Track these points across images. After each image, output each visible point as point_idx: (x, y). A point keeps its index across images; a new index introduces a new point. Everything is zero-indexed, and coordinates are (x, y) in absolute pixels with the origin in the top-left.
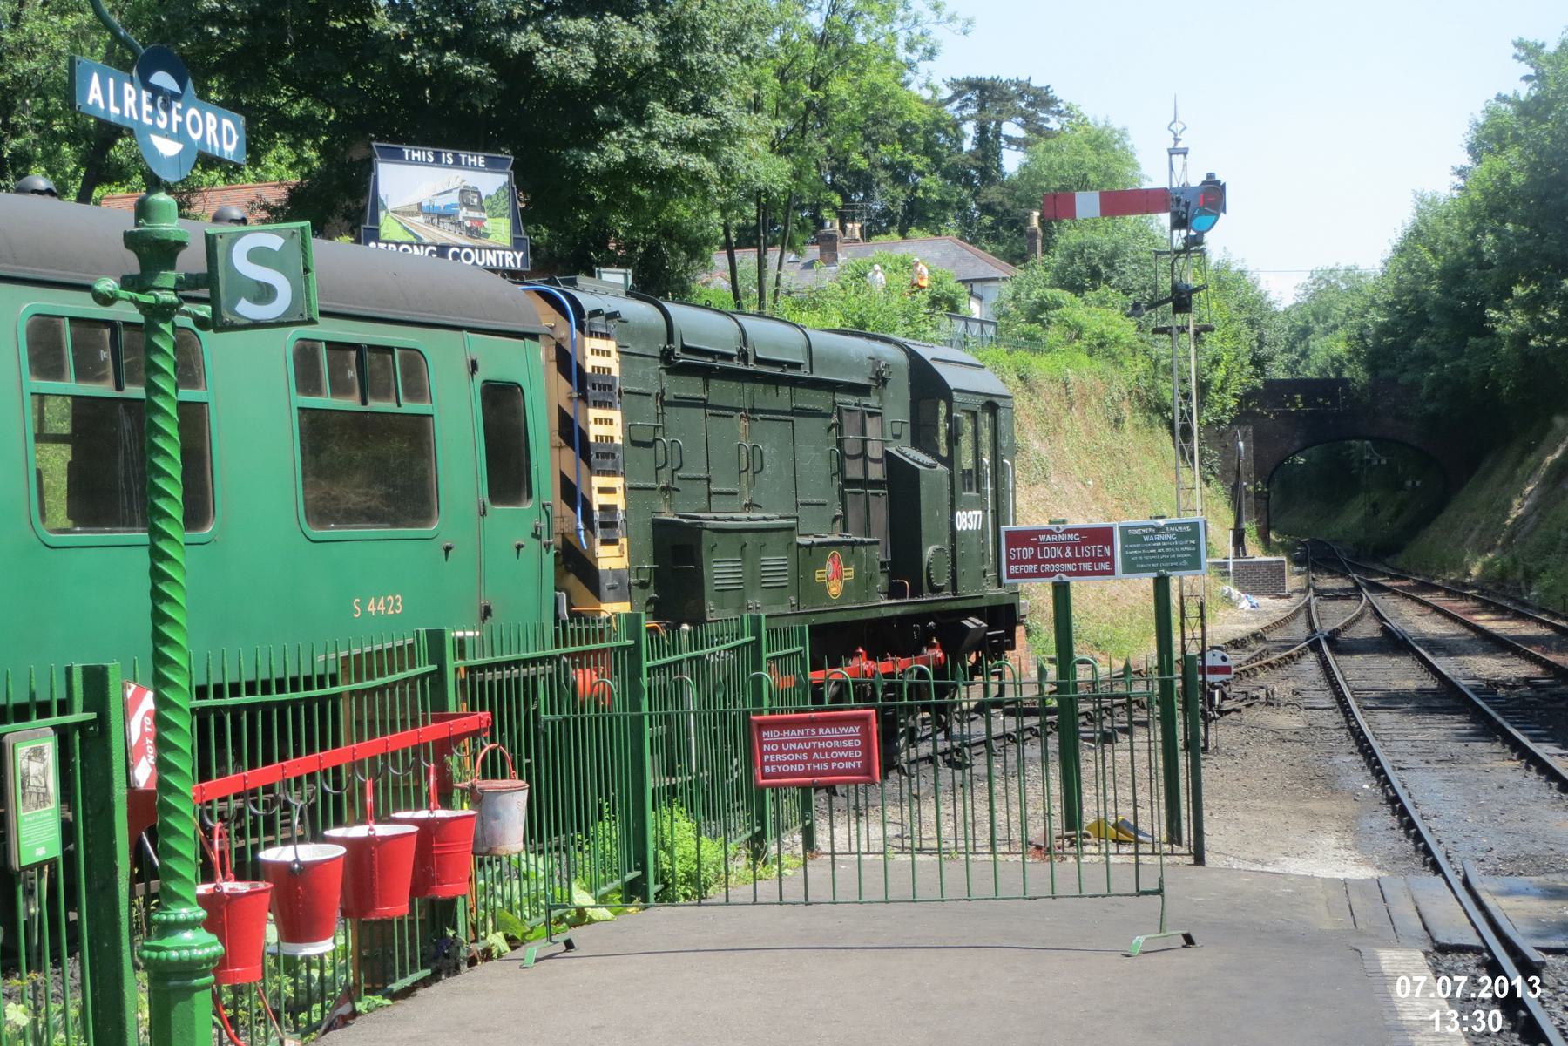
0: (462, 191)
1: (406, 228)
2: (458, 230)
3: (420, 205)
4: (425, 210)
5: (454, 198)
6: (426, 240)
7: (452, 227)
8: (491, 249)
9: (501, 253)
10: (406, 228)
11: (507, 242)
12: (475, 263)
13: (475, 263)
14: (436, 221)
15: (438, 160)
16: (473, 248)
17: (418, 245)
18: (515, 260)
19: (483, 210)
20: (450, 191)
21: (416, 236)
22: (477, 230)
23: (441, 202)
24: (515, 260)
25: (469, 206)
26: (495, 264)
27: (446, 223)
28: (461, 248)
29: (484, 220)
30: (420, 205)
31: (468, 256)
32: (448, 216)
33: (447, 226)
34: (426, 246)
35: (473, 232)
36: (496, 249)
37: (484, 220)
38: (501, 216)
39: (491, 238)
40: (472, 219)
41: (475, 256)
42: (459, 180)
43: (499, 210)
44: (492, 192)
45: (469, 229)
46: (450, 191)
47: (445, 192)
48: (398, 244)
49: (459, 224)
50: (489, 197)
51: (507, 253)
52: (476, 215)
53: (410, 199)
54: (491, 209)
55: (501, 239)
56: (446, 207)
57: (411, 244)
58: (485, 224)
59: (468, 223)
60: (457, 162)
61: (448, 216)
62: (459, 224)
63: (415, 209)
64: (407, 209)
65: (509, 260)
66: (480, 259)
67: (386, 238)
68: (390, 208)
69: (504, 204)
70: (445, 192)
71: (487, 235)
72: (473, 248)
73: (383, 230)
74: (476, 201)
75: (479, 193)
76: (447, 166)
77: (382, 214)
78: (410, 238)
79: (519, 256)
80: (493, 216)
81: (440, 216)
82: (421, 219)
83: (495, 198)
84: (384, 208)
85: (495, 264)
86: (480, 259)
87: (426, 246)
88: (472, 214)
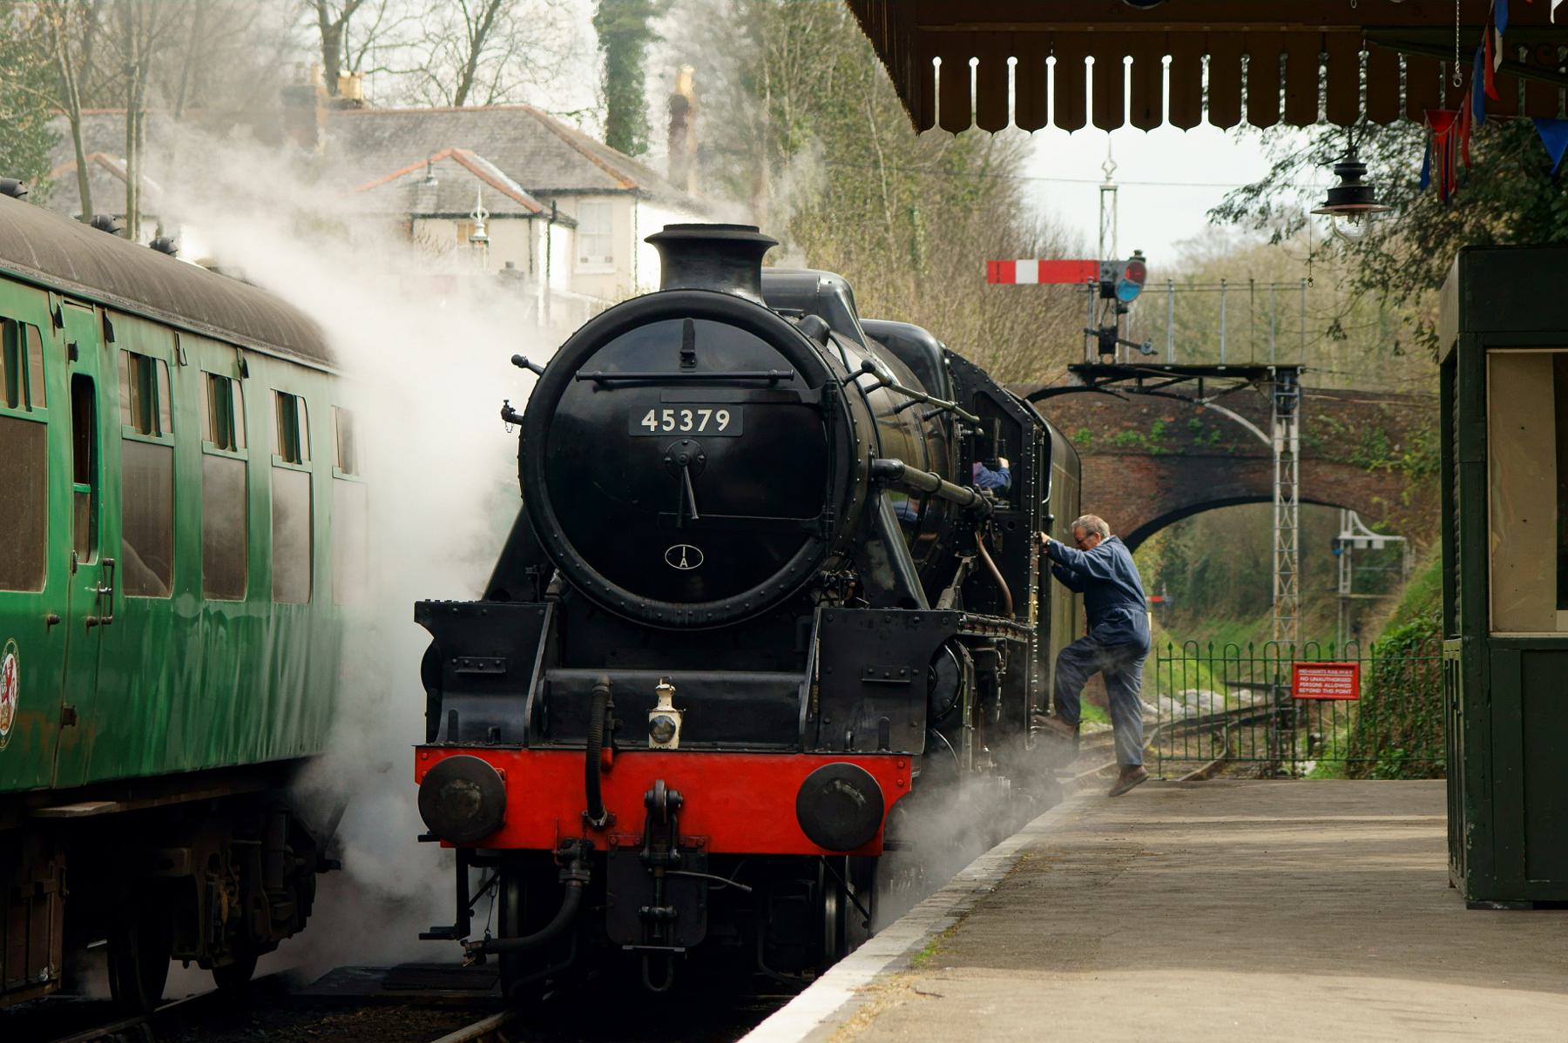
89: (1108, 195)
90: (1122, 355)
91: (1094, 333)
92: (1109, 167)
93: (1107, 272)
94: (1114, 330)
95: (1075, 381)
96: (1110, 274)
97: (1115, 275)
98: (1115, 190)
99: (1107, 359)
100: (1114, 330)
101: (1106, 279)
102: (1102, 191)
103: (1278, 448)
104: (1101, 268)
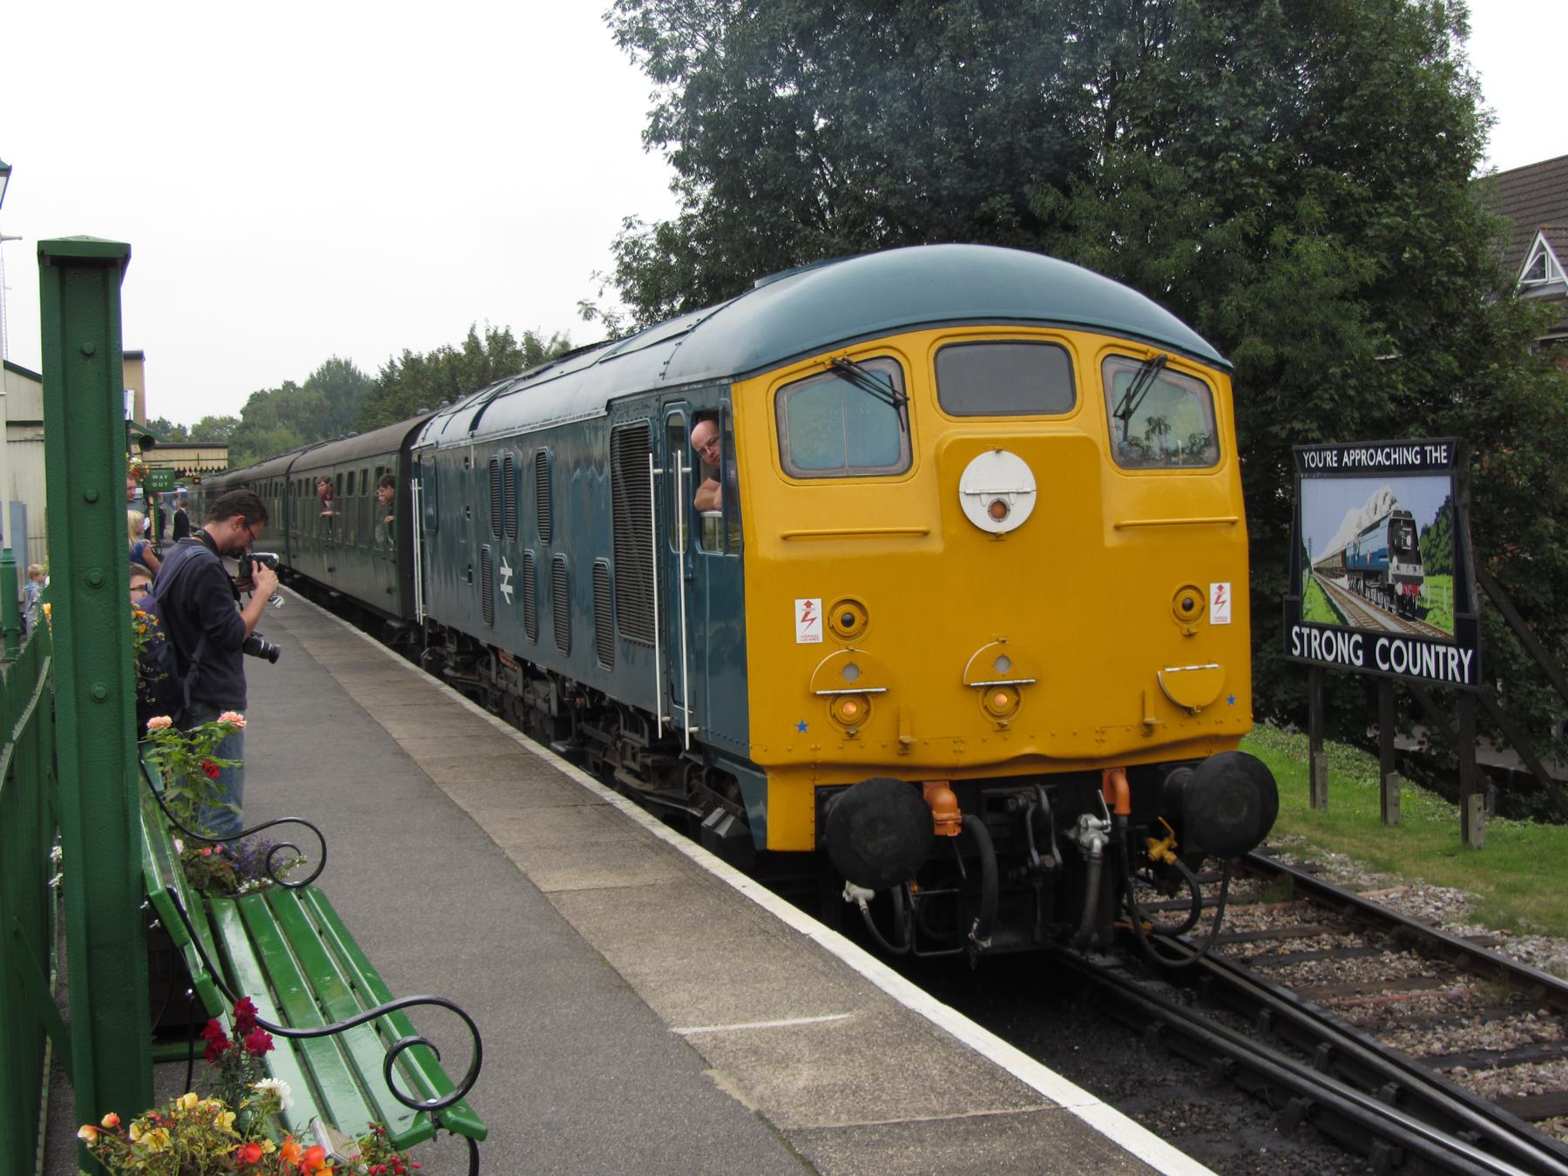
0: (1393, 523)
6: (1352, 623)
7: (1381, 598)
8: (1430, 642)
9: (1441, 649)
16: (1405, 639)
19: (1419, 562)
21: (1340, 616)
24: (1460, 665)
28: (1392, 637)
29: (1419, 581)
30: (1344, 553)
38: (1443, 570)
41: (1408, 657)
42: (1388, 501)
48: (1322, 629)
49: (1389, 590)
50: (1426, 531)
51: (1452, 651)
54: (1429, 556)
56: (1373, 555)
58: (1422, 588)
62: (1389, 590)
63: (1338, 563)
67: (1308, 619)
68: (1314, 561)
71: (1423, 613)
72: (1405, 639)
73: (1307, 606)
74: (1409, 540)
75: (1412, 524)
78: (1331, 618)
82: (1344, 582)
83: (1433, 534)
84: (1308, 563)
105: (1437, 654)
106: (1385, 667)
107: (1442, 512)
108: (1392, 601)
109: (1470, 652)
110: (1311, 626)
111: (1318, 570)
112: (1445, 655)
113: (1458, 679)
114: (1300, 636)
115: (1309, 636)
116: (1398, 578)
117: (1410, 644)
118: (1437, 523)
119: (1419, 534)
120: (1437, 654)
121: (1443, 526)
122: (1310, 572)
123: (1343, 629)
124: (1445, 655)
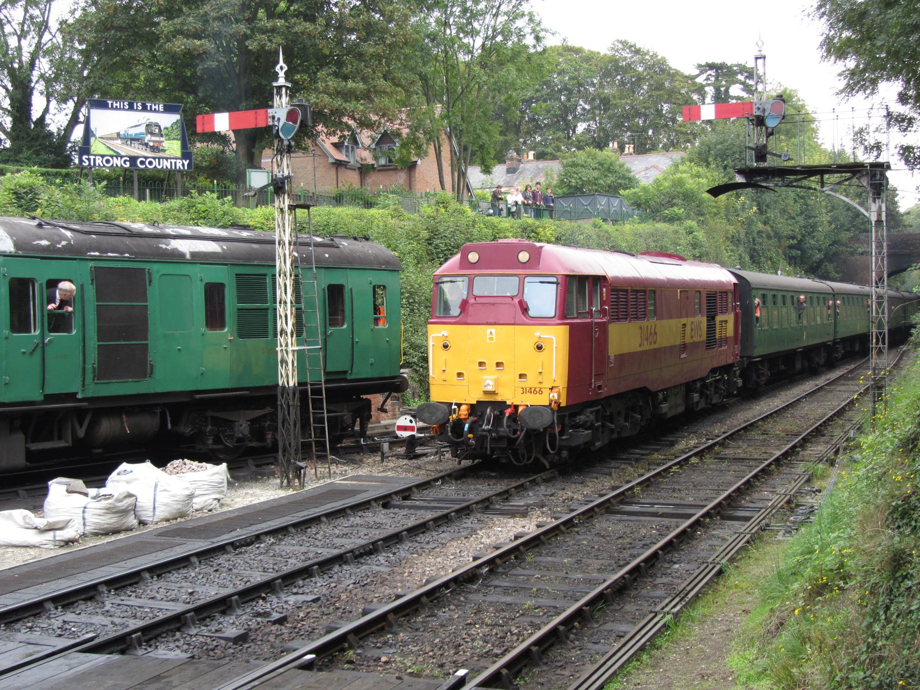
1: (108, 147)
2: (144, 147)
3: (118, 134)
4: (122, 136)
5: (142, 129)
6: (123, 154)
7: (141, 146)
8: (167, 159)
9: (173, 161)
10: (108, 147)
11: (179, 154)
12: (155, 167)
13: (155, 167)
14: (129, 142)
15: (131, 108)
16: (154, 158)
17: (117, 157)
18: (183, 165)
19: (162, 136)
20: (139, 125)
21: (115, 152)
22: (157, 148)
23: (133, 132)
24: (183, 165)
25: (152, 134)
26: (169, 167)
27: (136, 144)
28: (146, 158)
29: (163, 142)
31: (151, 163)
32: (137, 140)
33: (137, 145)
34: (122, 157)
35: (154, 149)
36: (170, 158)
37: (163, 142)
38: (174, 139)
39: (167, 152)
40: (154, 142)
42: (146, 119)
43: (173, 136)
44: (169, 125)
45: (151, 147)
46: (139, 125)
47: (136, 126)
48: (103, 156)
49: (146, 145)
50: (166, 128)
51: (178, 161)
52: (157, 139)
53: (112, 130)
54: (167, 135)
55: (174, 153)
57: (112, 156)
58: (163, 144)
59: (151, 144)
60: (144, 108)
61: (137, 140)
62: (146, 145)
64: (110, 136)
65: (179, 165)
66: (159, 164)
67: (95, 153)
68: (97, 136)
69: (177, 132)
70: (136, 126)
71: (164, 151)
72: (154, 158)
74: (157, 131)
75: (159, 127)
76: (137, 110)
77: (92, 140)
79: (186, 163)
80: (169, 139)
81: (132, 140)
82: (119, 141)
83: (170, 129)
84: (94, 135)
85: (169, 167)
86: (159, 164)
87: (122, 157)
88: (154, 138)
89: (760, 62)
90: (771, 162)
91: (750, 148)
92: (760, 43)
93: (759, 109)
94: (765, 146)
95: (739, 179)
96: (761, 110)
97: (764, 110)
98: (764, 58)
99: (763, 165)
100: (765, 146)
101: (758, 113)
102: (757, 58)
103: (874, 218)
104: (755, 107)
105: (171, 162)
106: (144, 166)
107: (176, 123)
108: (147, 147)
109: (188, 161)
110: (95, 155)
111: (101, 138)
112: (175, 163)
113: (182, 168)
114: (89, 160)
115: (94, 160)
116: (150, 141)
117: (157, 160)
118: (172, 127)
119: (162, 129)
120: (171, 162)
121: (175, 127)
122: (96, 138)
123: (118, 156)
124: (175, 163)
